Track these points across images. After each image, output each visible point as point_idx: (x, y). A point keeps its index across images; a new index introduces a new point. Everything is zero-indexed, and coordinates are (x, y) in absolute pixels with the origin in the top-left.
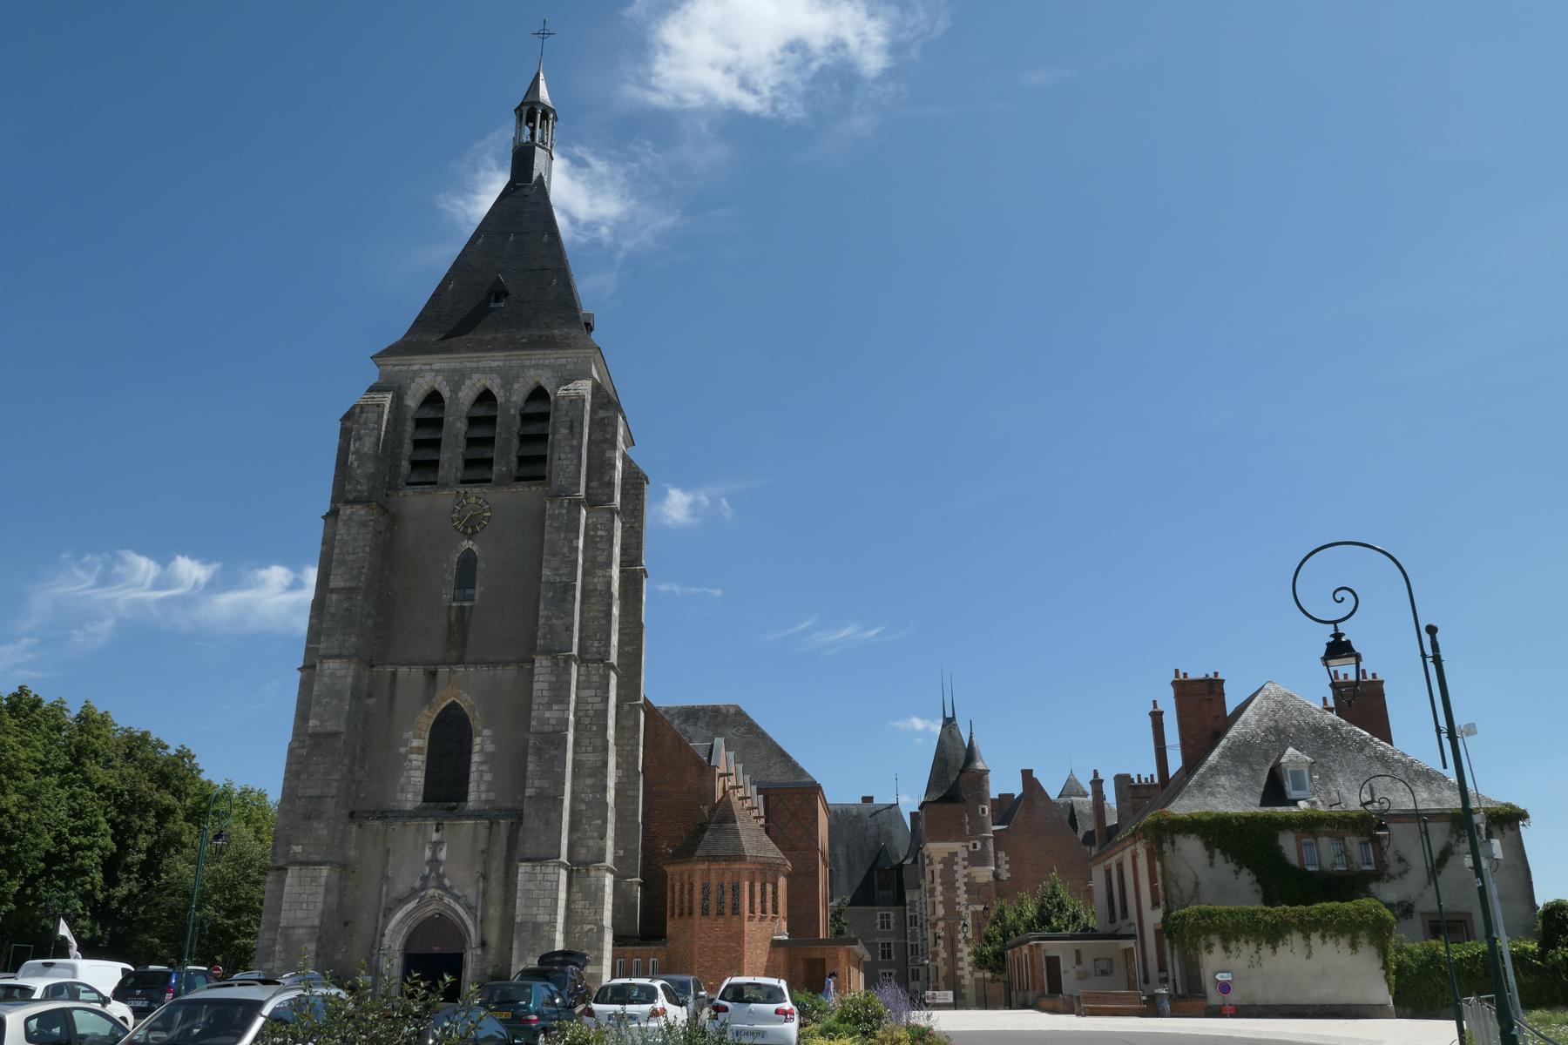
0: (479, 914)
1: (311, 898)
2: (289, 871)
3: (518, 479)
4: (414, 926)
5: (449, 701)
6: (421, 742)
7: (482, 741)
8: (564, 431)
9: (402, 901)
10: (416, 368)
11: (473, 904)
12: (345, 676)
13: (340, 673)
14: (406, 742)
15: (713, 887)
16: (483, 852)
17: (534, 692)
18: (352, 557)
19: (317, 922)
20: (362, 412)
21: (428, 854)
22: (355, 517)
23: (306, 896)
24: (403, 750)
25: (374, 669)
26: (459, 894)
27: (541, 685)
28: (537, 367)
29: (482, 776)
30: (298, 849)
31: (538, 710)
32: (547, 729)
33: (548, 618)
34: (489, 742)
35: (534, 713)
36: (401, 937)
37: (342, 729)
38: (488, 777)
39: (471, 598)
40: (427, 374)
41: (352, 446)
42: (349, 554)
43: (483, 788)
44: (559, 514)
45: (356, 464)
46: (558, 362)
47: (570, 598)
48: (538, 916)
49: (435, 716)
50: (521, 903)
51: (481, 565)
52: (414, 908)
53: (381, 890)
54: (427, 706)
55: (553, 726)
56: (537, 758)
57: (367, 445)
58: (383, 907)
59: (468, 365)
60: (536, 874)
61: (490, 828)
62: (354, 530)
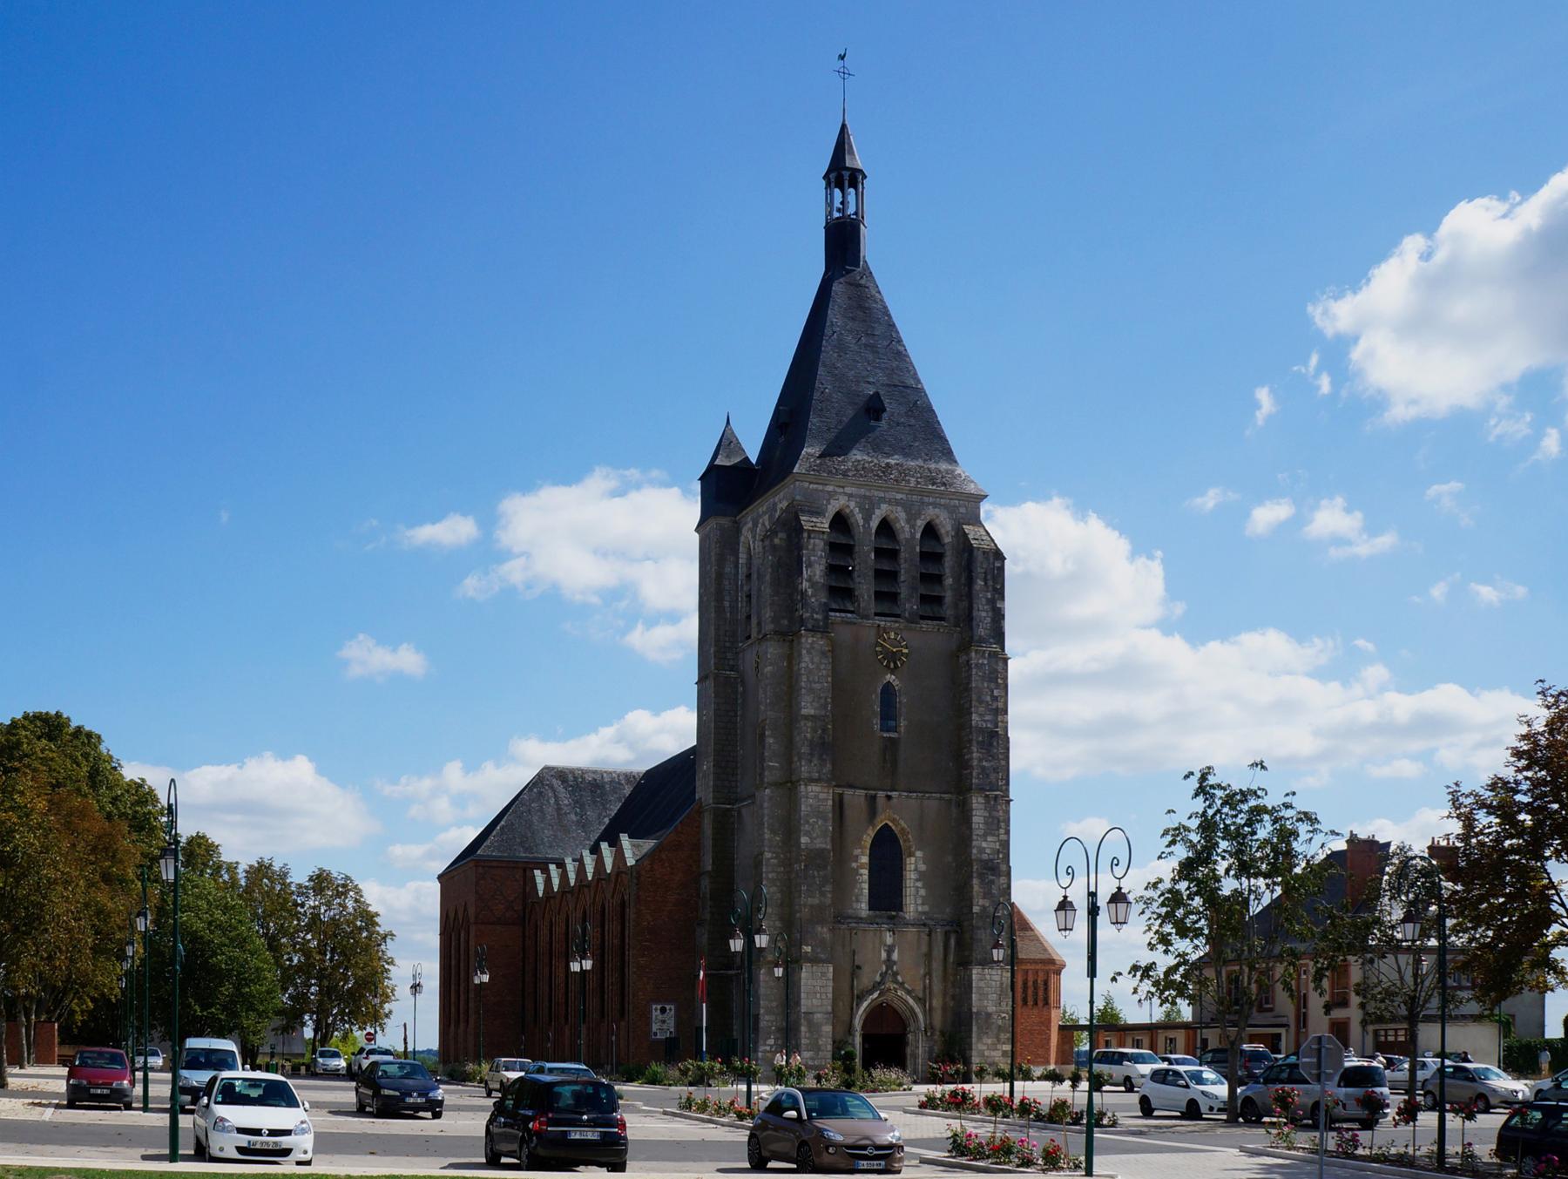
3: (923, 618)
6: (865, 859)
7: (916, 861)
8: (981, 583)
9: (870, 992)
10: (830, 488)
11: (921, 995)
13: (822, 796)
14: (856, 858)
15: (1030, 984)
16: (926, 955)
18: (817, 686)
20: (809, 537)
21: (884, 955)
22: (815, 646)
24: (854, 865)
26: (910, 988)
27: (978, 819)
28: (935, 505)
29: (918, 891)
30: (809, 949)
31: (977, 840)
32: (985, 857)
33: (980, 760)
35: (974, 843)
38: (922, 892)
39: (895, 729)
40: (841, 497)
41: (805, 572)
42: (815, 683)
43: (919, 901)
44: (983, 664)
45: (810, 592)
46: (952, 502)
47: (995, 744)
51: (903, 699)
55: (988, 854)
57: (818, 572)
59: (876, 493)
61: (929, 935)
62: (816, 659)
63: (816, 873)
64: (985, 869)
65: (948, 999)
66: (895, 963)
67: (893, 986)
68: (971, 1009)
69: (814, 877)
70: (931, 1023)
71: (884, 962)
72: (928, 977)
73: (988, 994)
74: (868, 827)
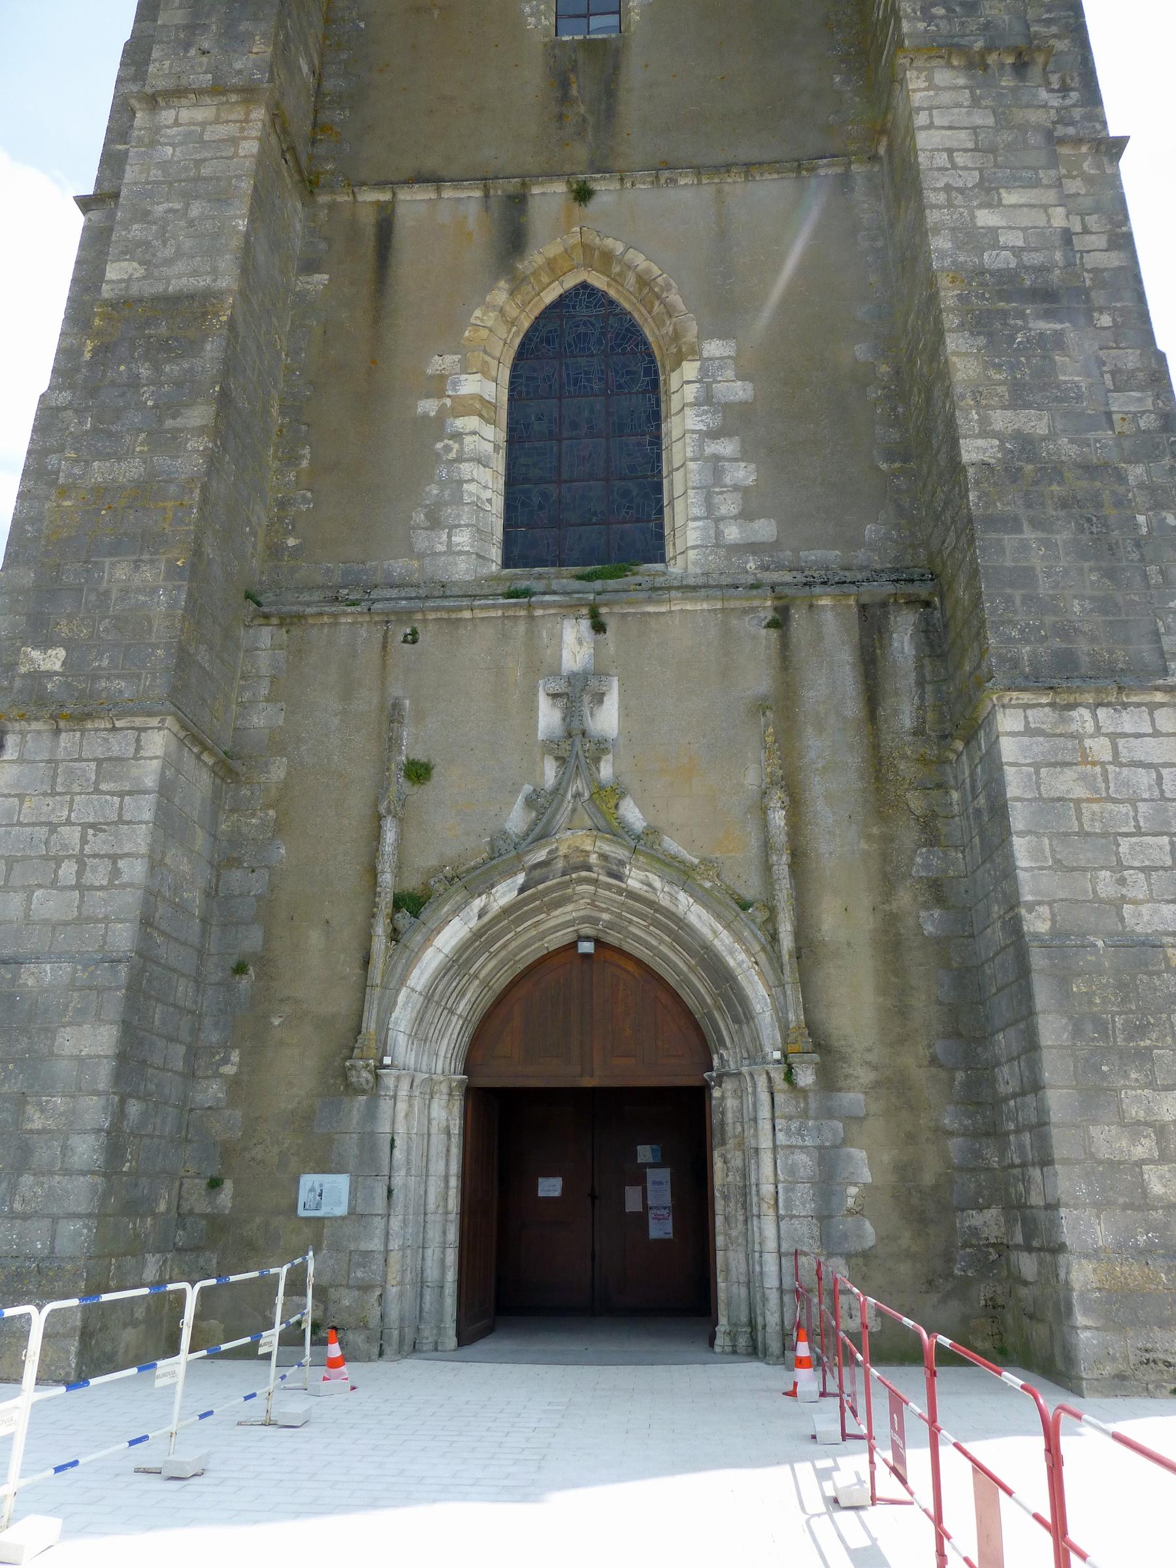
0: (786, 929)
1: (97, 843)
2: (11, 740)
4: (502, 981)
5: (571, 282)
7: (703, 371)
11: (751, 888)
12: (234, 141)
14: (438, 385)
17: (922, 158)
19: (123, 937)
21: (548, 717)
23: (76, 832)
24: (428, 407)
25: (323, 199)
34: (730, 373)
36: (456, 1024)
37: (223, 283)
38: (742, 474)
43: (728, 506)
48: (1127, 909)
49: (526, 325)
50: (1036, 853)
52: (506, 911)
53: (377, 836)
54: (502, 284)
55: (1017, 251)
56: (981, 341)
58: (385, 902)
60: (1078, 737)
63: (144, 371)
64: (1003, 295)
65: (904, 899)
66: (601, 747)
67: (594, 847)
68: (1014, 927)
69: (134, 383)
70: (811, 1027)
71: (550, 746)
72: (777, 798)
73: (1111, 837)
74: (496, 279)
